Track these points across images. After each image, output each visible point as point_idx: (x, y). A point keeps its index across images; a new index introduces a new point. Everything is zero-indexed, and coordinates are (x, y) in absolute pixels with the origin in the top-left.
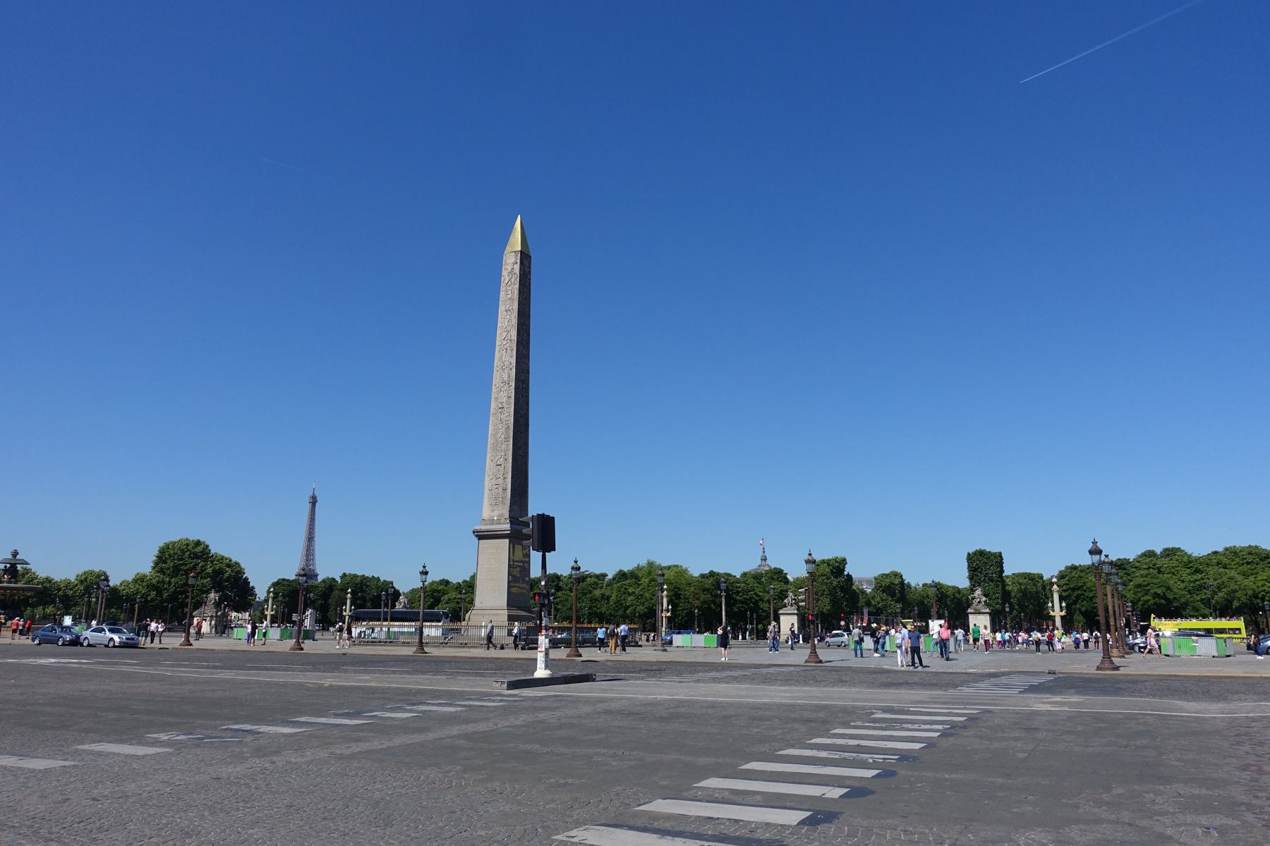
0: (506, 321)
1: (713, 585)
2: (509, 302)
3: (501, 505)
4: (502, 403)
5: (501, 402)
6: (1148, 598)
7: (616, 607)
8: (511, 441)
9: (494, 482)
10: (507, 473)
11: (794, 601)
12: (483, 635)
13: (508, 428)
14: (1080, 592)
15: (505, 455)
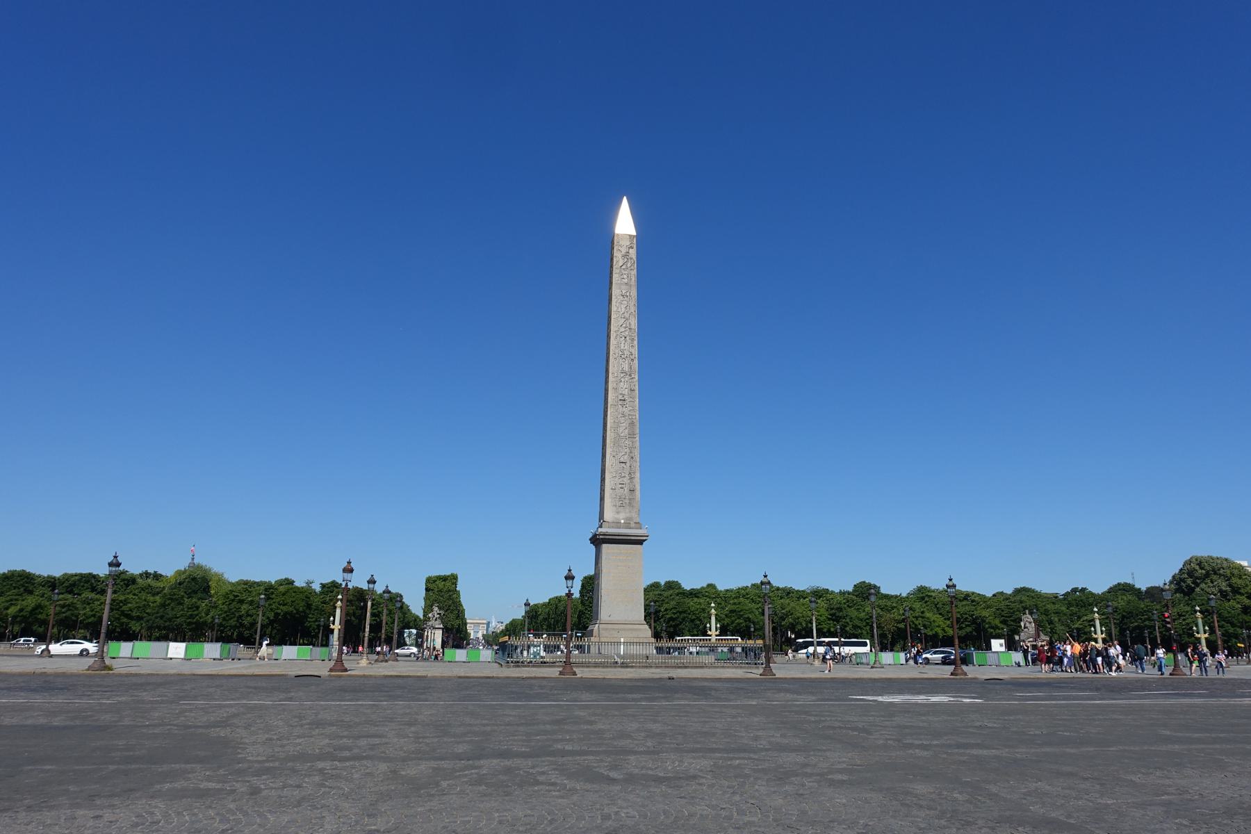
0: (623, 306)
1: (356, 596)
2: (623, 287)
3: (628, 507)
4: (623, 395)
5: (621, 394)
6: (741, 621)
7: (227, 616)
8: (637, 438)
9: (618, 481)
10: (634, 473)
11: (438, 616)
12: (622, 653)
13: (632, 424)
14: (685, 615)
15: (631, 452)
